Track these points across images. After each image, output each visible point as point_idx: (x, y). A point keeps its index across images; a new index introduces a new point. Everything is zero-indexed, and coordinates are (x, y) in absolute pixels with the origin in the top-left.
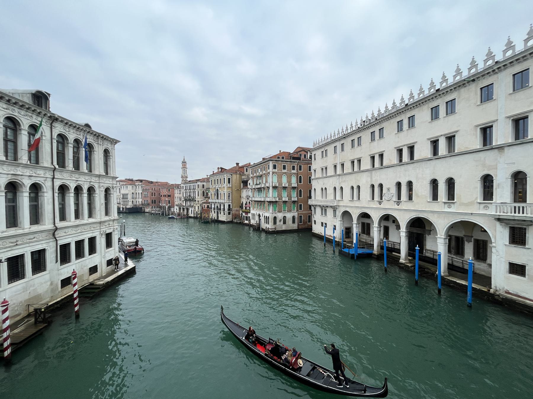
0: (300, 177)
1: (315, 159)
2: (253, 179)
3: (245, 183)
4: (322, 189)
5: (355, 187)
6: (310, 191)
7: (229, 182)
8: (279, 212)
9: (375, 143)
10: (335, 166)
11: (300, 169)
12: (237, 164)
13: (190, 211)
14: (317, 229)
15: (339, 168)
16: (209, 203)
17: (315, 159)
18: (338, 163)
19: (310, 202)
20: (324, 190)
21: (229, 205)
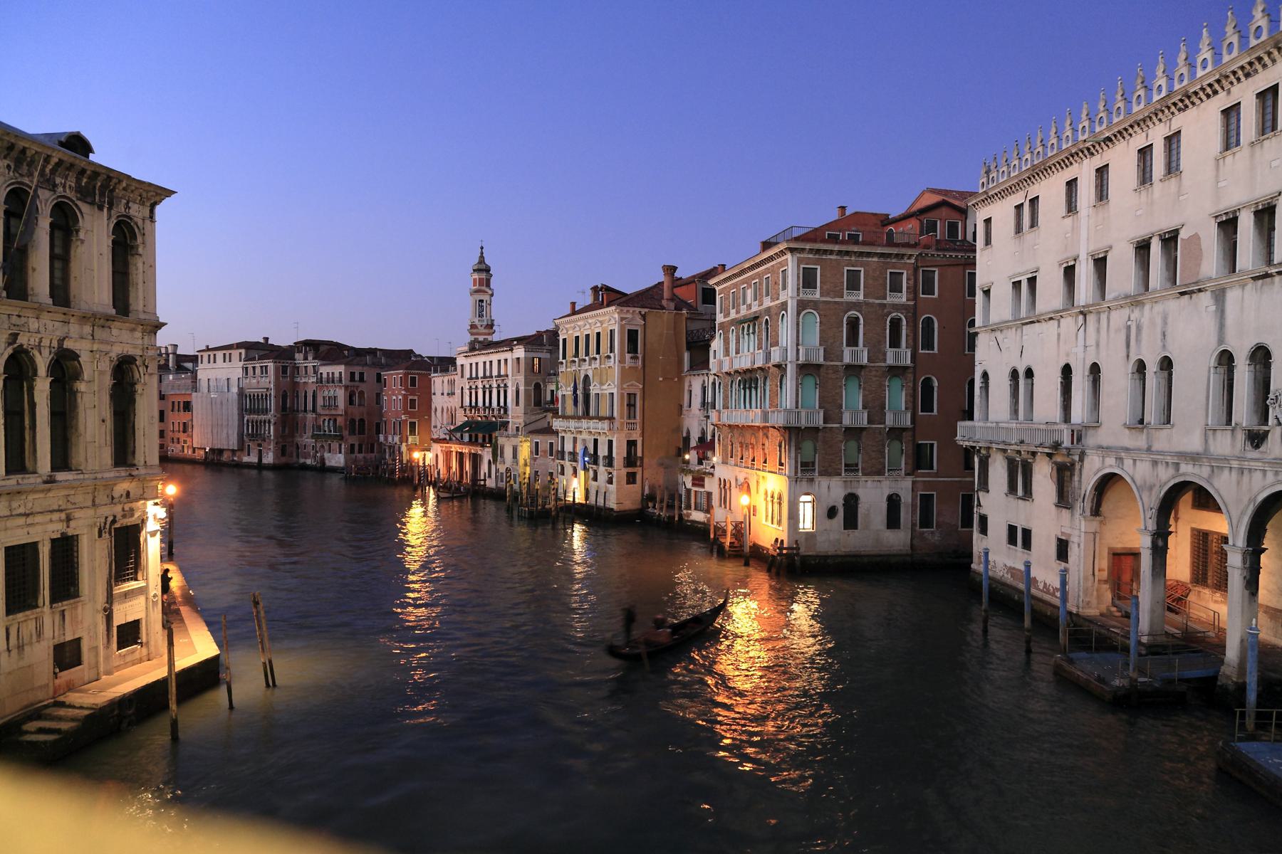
0: (928, 322)
1: (988, 242)
2: (726, 333)
3: (699, 350)
4: (1014, 374)
5: (1152, 367)
6: (972, 382)
7: (633, 348)
9: (1239, 158)
10: (1069, 272)
11: (929, 289)
12: (670, 270)
13: (484, 468)
14: (994, 555)
15: (1085, 273)
16: (557, 433)
17: (988, 242)
18: (1083, 257)
19: (966, 433)
20: (1022, 378)
21: (631, 444)
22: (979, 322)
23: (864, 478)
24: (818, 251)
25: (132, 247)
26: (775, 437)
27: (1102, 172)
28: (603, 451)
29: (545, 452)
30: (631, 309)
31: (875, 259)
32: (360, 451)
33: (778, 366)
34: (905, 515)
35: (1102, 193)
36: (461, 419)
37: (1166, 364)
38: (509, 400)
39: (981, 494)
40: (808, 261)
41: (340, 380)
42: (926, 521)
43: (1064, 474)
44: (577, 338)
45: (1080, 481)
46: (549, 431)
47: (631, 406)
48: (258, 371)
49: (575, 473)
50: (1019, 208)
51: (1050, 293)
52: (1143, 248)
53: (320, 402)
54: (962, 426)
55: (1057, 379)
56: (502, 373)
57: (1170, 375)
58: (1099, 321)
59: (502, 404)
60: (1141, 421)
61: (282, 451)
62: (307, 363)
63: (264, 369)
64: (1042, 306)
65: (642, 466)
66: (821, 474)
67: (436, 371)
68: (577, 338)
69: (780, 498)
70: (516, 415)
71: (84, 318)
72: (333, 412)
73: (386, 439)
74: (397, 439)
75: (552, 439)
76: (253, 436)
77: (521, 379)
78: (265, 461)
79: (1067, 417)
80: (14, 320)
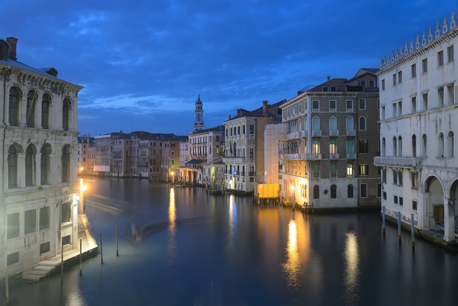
0: (362, 119)
1: (383, 89)
4: (395, 138)
5: (446, 135)
8: (325, 176)
10: (414, 100)
11: (362, 106)
13: (198, 177)
14: (389, 207)
15: (419, 100)
16: (224, 163)
17: (383, 89)
19: (377, 161)
20: (398, 140)
22: (381, 119)
23: (338, 179)
24: (319, 95)
25: (70, 107)
26: (304, 164)
27: (425, 61)
28: (241, 170)
29: (220, 170)
30: (251, 118)
31: (341, 96)
32: (154, 171)
33: (304, 138)
34: (355, 193)
35: (425, 69)
36: (190, 159)
37: (451, 134)
38: (207, 151)
39: (384, 184)
40: (315, 98)
41: (147, 146)
42: (364, 194)
43: (414, 176)
44: (231, 129)
45: (420, 179)
46: (221, 163)
47: (251, 153)
48: (118, 143)
49: (231, 179)
50: (395, 75)
51: (407, 107)
52: (441, 90)
53: (140, 154)
54: (376, 158)
55: (411, 140)
56: (205, 142)
57: (453, 138)
58: (425, 118)
59: (205, 153)
60: (443, 156)
61: (126, 172)
62: (135, 140)
63: (120, 142)
64: (404, 112)
65: (256, 175)
66: (321, 178)
67: (181, 141)
68: (231, 129)
69: (306, 186)
70: (210, 157)
71: (53, 133)
72: (144, 157)
73: (163, 166)
74: (167, 166)
75: (223, 166)
76: (117, 166)
77: (211, 144)
78: (120, 175)
79: (415, 155)
80: (30, 134)
